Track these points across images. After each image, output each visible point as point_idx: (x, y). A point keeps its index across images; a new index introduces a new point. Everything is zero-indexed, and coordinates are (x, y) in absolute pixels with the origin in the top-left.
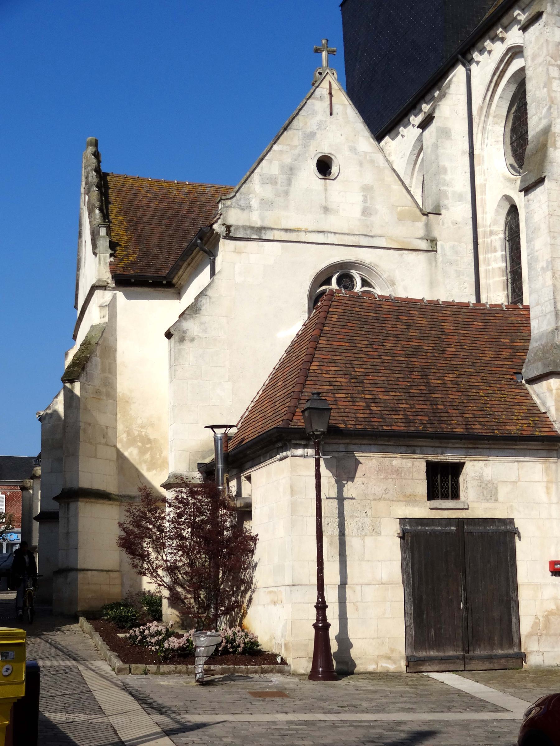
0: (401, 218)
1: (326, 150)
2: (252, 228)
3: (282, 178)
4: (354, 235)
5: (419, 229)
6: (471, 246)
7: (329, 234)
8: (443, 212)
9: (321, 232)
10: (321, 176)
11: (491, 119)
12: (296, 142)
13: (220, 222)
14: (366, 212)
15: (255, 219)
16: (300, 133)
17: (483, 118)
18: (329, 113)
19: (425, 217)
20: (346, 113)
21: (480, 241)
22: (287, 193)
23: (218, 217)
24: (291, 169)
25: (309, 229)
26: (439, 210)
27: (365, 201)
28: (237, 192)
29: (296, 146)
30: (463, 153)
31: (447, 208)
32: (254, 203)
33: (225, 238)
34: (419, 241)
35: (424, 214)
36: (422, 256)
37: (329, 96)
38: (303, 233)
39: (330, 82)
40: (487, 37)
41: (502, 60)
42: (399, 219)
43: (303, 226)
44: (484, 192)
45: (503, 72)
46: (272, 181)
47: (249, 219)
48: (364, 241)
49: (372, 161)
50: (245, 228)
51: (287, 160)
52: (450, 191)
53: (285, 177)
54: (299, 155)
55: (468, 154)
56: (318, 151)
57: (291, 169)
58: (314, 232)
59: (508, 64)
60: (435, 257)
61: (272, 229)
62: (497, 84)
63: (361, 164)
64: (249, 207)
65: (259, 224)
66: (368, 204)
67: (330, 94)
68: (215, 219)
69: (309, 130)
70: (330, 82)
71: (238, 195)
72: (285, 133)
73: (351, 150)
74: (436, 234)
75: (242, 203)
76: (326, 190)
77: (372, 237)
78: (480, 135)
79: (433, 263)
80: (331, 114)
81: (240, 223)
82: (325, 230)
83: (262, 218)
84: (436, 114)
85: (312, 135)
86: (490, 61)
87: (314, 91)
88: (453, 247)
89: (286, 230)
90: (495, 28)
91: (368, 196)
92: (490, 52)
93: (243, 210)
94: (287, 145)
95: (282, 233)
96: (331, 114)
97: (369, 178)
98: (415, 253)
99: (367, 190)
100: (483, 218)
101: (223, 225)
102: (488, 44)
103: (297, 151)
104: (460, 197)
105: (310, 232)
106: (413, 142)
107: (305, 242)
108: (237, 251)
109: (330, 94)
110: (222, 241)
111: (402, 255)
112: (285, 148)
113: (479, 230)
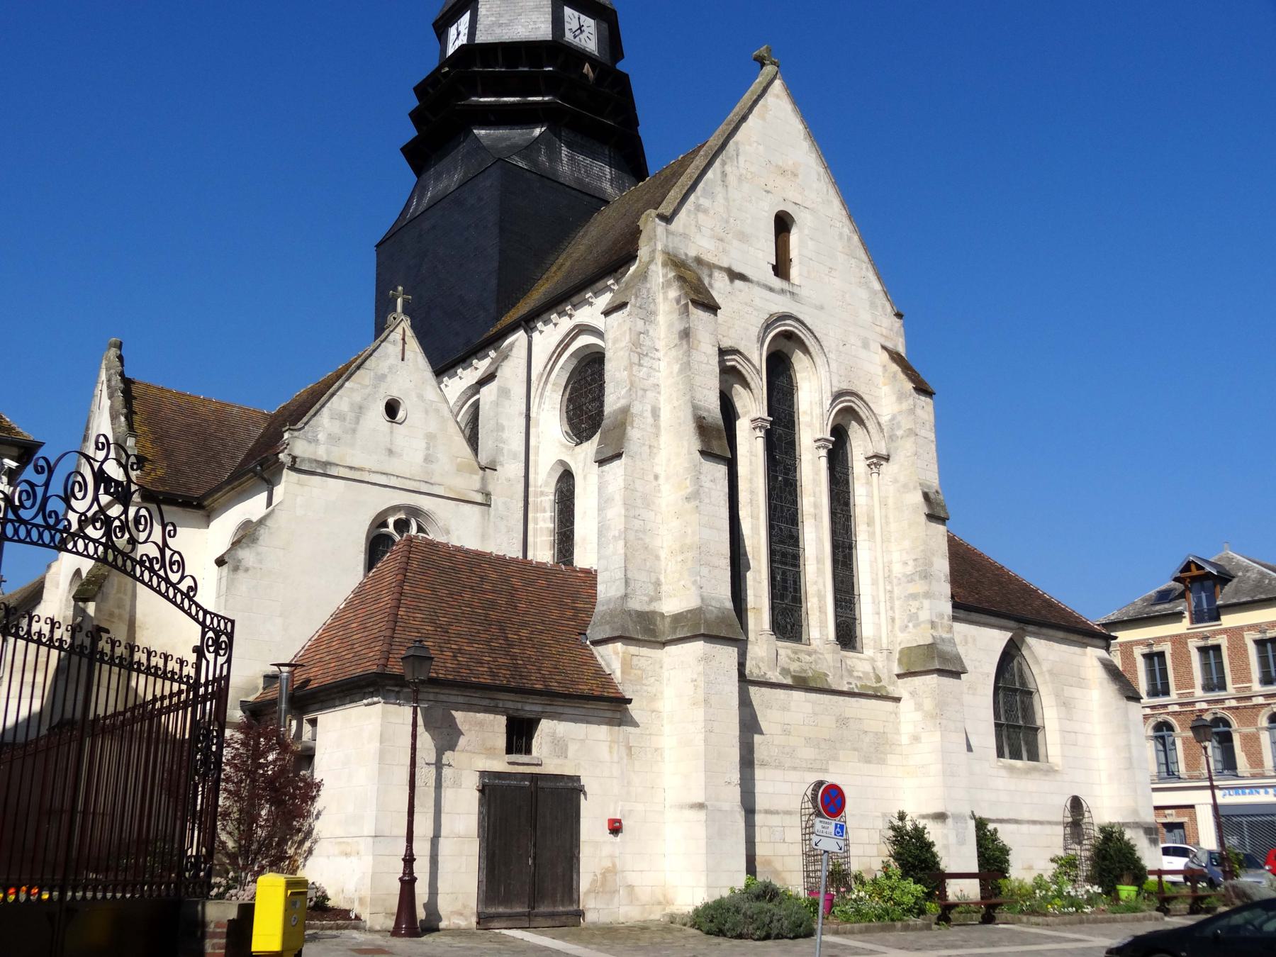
0: (460, 469)
1: (395, 393)
2: (317, 462)
3: (350, 416)
4: (415, 480)
5: (475, 480)
6: (521, 504)
7: (392, 477)
8: (498, 468)
9: (384, 474)
10: (388, 419)
11: (549, 386)
12: (367, 382)
13: (286, 451)
14: (428, 459)
15: (322, 453)
16: (372, 374)
17: (542, 384)
18: (400, 358)
19: (481, 472)
20: (417, 362)
21: (531, 500)
22: (354, 431)
23: (285, 446)
24: (361, 408)
25: (373, 470)
26: (495, 466)
27: (428, 448)
28: (306, 424)
29: (368, 386)
30: (521, 414)
31: (502, 465)
32: (321, 437)
33: (289, 468)
34: (475, 493)
35: (481, 468)
36: (476, 508)
37: (402, 342)
38: (367, 473)
39: (404, 329)
40: (554, 310)
41: (568, 335)
42: (458, 470)
43: (367, 466)
44: (537, 454)
45: (567, 345)
46: (341, 417)
47: (316, 452)
48: (424, 488)
49: (437, 411)
50: (311, 461)
51: (357, 398)
52: (506, 447)
53: (353, 415)
54: (369, 395)
55: (524, 415)
56: (388, 393)
57: (361, 408)
58: (377, 472)
59: (573, 339)
60: (488, 510)
61: (337, 465)
62: (560, 355)
63: (427, 412)
64: (317, 441)
65: (324, 459)
66: (430, 452)
67: (403, 339)
68: (282, 448)
69: (380, 372)
70: (404, 329)
71: (306, 427)
72: (358, 372)
73: (418, 397)
74: (490, 488)
75: (310, 435)
76: (391, 432)
77: (432, 484)
78: (537, 400)
79: (486, 517)
80: (403, 360)
81: (306, 455)
82: (389, 472)
83: (328, 452)
84: (498, 374)
85: (382, 377)
86: (554, 333)
87: (388, 335)
88: (505, 503)
89: (351, 468)
90: (563, 304)
91: (431, 444)
92: (555, 325)
93: (310, 442)
94: (359, 383)
95: (347, 470)
96: (403, 360)
97: (433, 426)
98: (470, 505)
99: (430, 437)
100: (535, 478)
101: (290, 455)
102: (554, 317)
103: (367, 391)
104: (515, 457)
105: (374, 472)
106: (459, 394)
107: (368, 483)
108: (299, 483)
109: (403, 339)
110: (285, 471)
111: (458, 505)
112: (356, 386)
113: (531, 489)
